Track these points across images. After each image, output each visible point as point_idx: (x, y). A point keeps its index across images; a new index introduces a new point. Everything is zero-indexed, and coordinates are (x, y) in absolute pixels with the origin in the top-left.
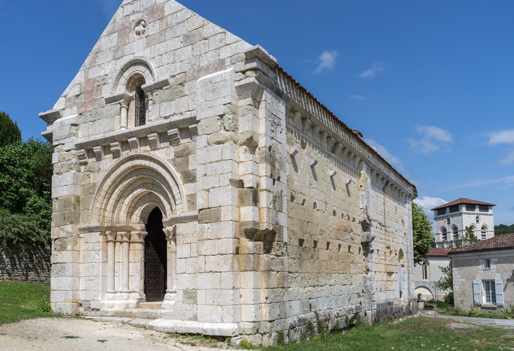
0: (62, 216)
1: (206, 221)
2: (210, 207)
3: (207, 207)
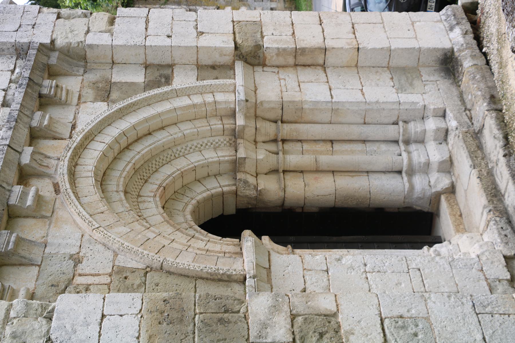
0: (212, 331)
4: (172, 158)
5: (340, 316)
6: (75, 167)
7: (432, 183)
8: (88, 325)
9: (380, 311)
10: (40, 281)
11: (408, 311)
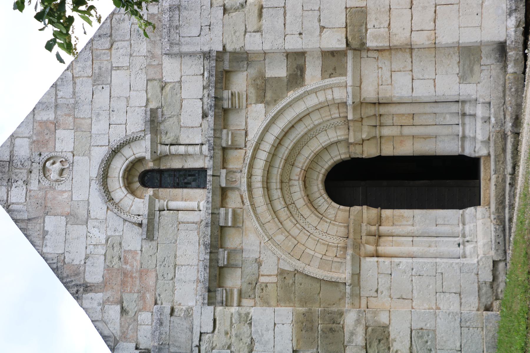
0: (327, 337)
1: (364, 31)
2: (344, 25)
3: (345, 29)
4: (308, 140)
5: (390, 328)
7: (477, 149)
8: (268, 331)
9: (411, 325)
10: (243, 280)
11: (426, 325)
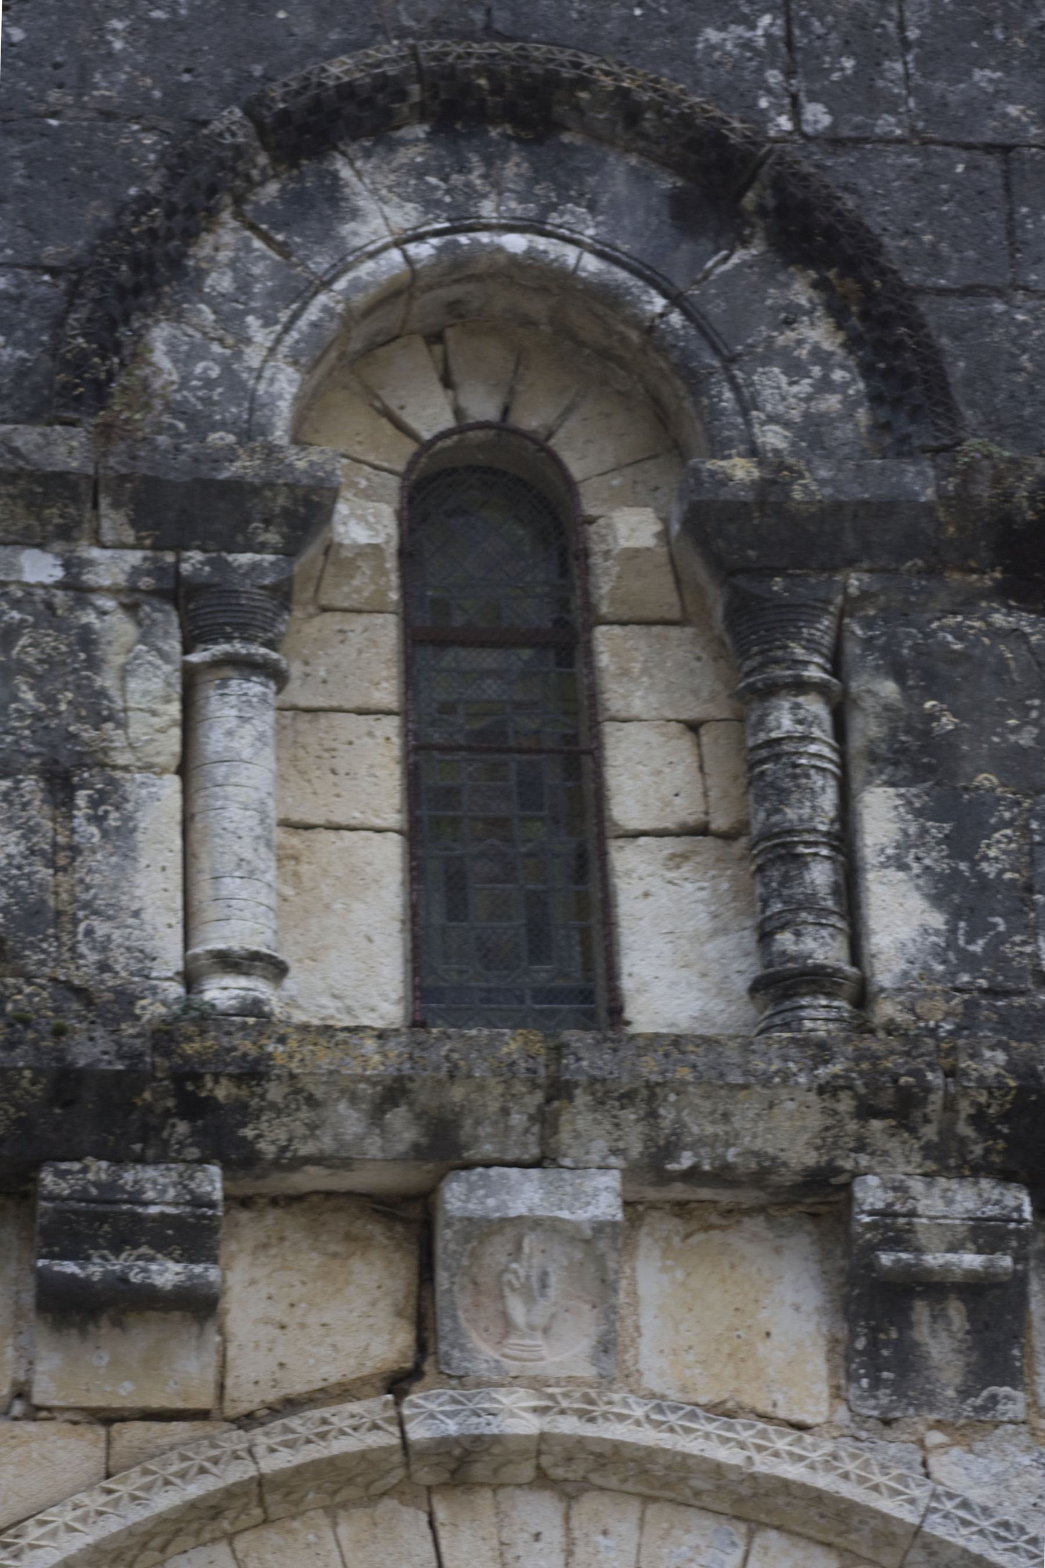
6: (543, 1480)
